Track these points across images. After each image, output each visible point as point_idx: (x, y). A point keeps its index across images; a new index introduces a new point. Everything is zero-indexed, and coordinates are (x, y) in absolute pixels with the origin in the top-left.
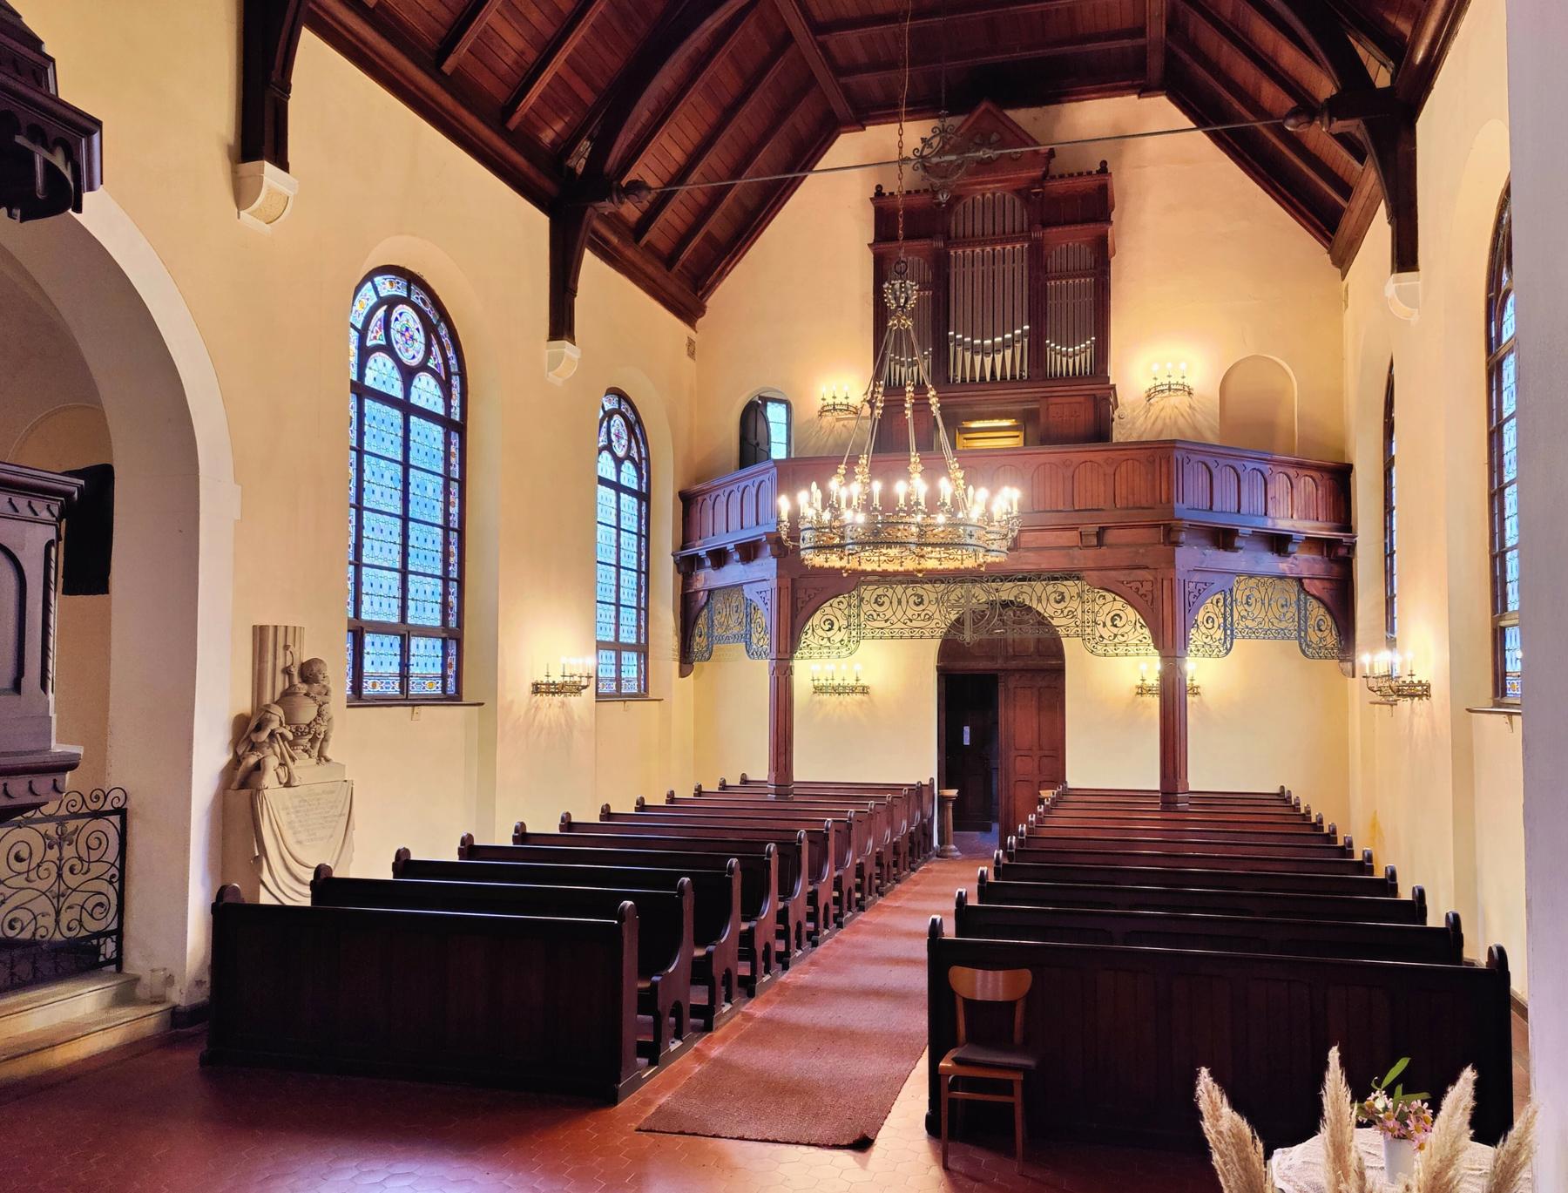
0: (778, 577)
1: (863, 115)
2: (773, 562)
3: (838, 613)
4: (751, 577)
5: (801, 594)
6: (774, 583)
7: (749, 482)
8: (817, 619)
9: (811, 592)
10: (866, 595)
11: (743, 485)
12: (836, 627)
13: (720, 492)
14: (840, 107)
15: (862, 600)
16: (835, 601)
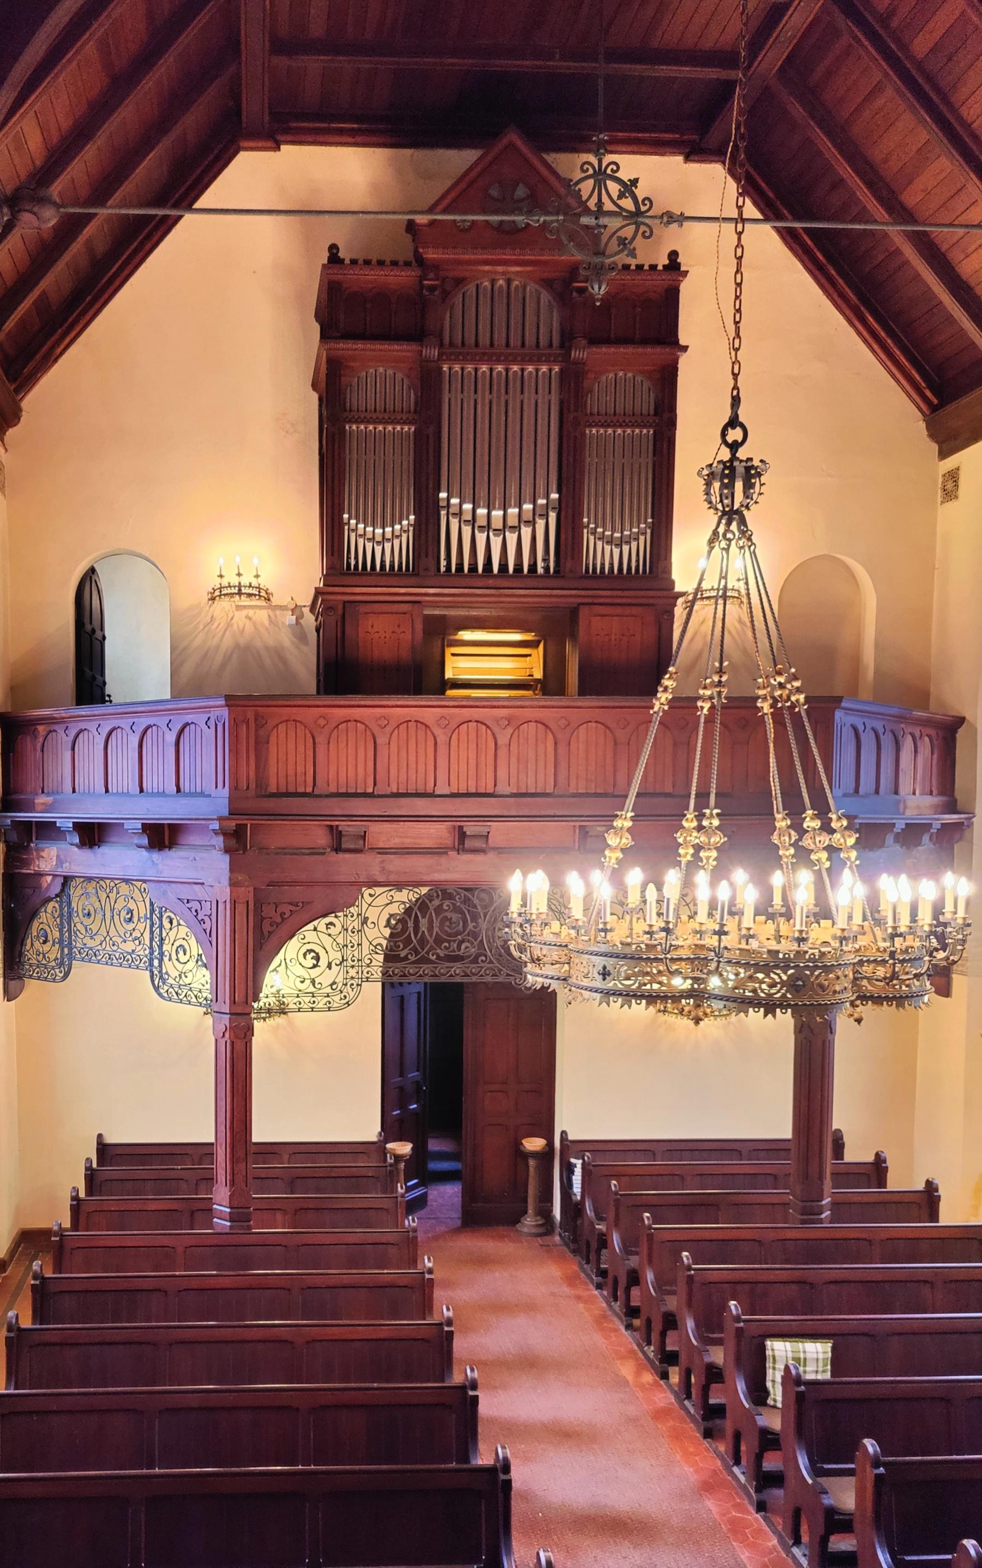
0: (233, 884)
1: (290, 121)
2: (222, 862)
3: (328, 942)
4: (167, 874)
5: (268, 911)
6: (223, 891)
7: (162, 721)
8: (292, 948)
9: (286, 909)
10: (372, 914)
11: (143, 722)
12: (323, 962)
13: (92, 726)
14: (254, 104)
15: (365, 921)
16: (321, 923)
